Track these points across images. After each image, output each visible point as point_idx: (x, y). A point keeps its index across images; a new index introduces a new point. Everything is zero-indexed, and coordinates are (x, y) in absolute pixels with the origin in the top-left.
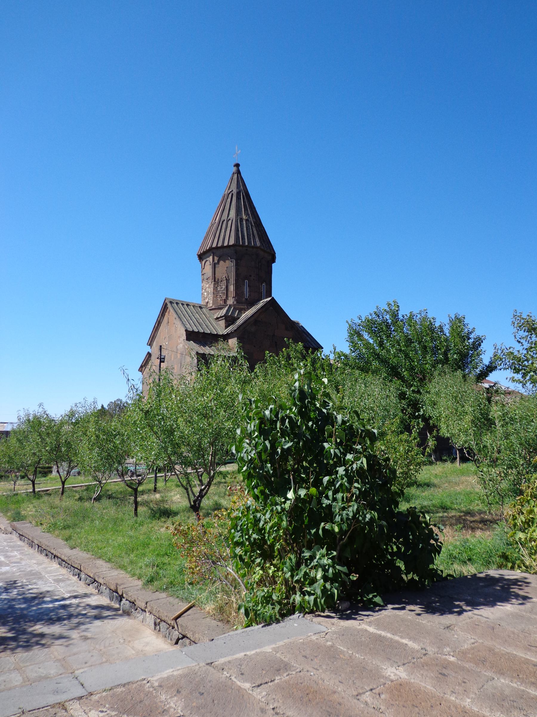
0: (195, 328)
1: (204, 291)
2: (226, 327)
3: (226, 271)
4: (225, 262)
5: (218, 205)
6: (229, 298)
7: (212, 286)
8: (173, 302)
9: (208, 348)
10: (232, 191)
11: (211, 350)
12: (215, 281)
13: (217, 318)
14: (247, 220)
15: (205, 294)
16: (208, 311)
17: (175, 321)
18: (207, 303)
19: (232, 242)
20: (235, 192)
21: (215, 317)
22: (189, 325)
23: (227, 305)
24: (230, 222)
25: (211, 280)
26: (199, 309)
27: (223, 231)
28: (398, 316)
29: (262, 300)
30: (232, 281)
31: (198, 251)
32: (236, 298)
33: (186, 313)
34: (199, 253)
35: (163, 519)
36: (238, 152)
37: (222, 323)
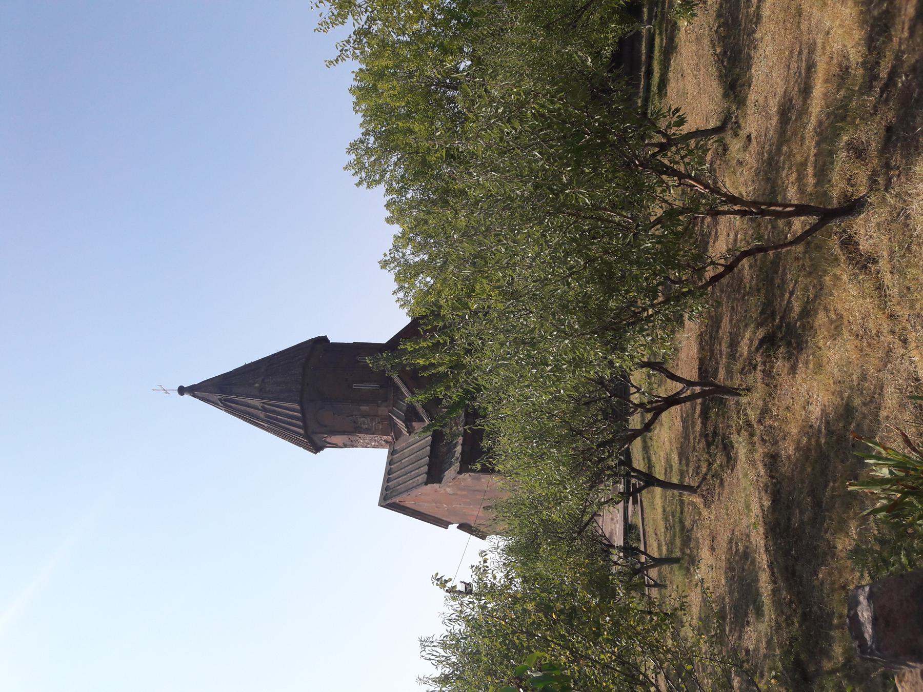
0: (422, 468)
8: (384, 494)
10: (220, 400)
18: (386, 442)
19: (297, 407)
22: (418, 478)
33: (400, 479)
37: (415, 424)
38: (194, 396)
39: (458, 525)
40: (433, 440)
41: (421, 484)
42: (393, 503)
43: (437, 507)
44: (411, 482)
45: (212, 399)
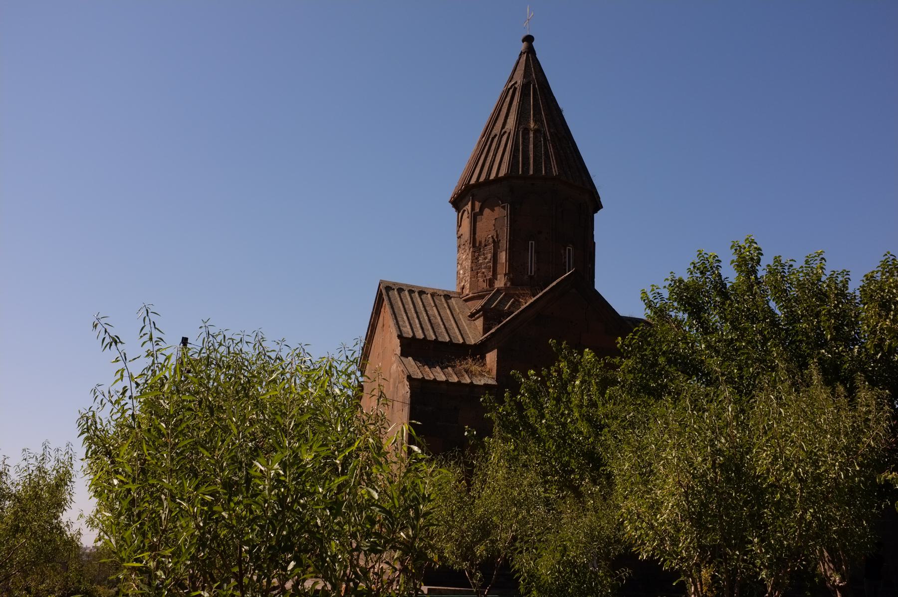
0: (420, 331)
1: (459, 266)
3: (494, 225)
4: (493, 210)
6: (499, 276)
8: (393, 287)
10: (516, 83)
12: (474, 246)
13: (472, 316)
14: (536, 131)
15: (461, 272)
18: (463, 288)
19: (502, 173)
22: (409, 327)
26: (443, 300)
27: (491, 154)
30: (504, 243)
32: (511, 275)
33: (411, 306)
36: (529, 16)
37: (479, 323)
41: (400, 331)
42: (383, 300)
44: (405, 318)
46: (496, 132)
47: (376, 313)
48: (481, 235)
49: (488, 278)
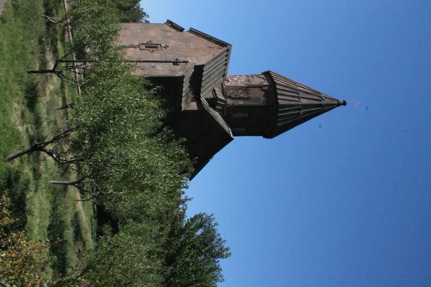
0: (206, 73)
1: (238, 77)
2: (207, 99)
3: (256, 97)
4: (264, 96)
5: (311, 88)
6: (232, 101)
7: (243, 85)
8: (228, 52)
9: (188, 85)
10: (324, 100)
11: (186, 88)
12: (247, 87)
13: (214, 91)
16: (221, 82)
17: (211, 54)
18: (228, 81)
19: (281, 102)
20: (323, 102)
21: (215, 89)
22: (208, 67)
23: (226, 99)
24: (297, 99)
25: (248, 84)
26: (222, 74)
27: (290, 94)
28: (218, 258)
29: (231, 129)
30: (247, 103)
31: (272, 71)
33: (219, 64)
34: (271, 73)
35: (26, 101)
36: (356, 104)
37: (210, 96)
38: (338, 101)
39: (184, 31)
40: (200, 89)
41: (206, 65)
42: (223, 47)
43: (197, 45)
44: (213, 64)
45: (327, 99)
46: (301, 94)
47: (216, 41)
48: (252, 90)
49: (232, 95)
